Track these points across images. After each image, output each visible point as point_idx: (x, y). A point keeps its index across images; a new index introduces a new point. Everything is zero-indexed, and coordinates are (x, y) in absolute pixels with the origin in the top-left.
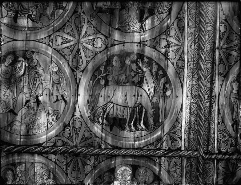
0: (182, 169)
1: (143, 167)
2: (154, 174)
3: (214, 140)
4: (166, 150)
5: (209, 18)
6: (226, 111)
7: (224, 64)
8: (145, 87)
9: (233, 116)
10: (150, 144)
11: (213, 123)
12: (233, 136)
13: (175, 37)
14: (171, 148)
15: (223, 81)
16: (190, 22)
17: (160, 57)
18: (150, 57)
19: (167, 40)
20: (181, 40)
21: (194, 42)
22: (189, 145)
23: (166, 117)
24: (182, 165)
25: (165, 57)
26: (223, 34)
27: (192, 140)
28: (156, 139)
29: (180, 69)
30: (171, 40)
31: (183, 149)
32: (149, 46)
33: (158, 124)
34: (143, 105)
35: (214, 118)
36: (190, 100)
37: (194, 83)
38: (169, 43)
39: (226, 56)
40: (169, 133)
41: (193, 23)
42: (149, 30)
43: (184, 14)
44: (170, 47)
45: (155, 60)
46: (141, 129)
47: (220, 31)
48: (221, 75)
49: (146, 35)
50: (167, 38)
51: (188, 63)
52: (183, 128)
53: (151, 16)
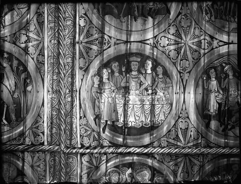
0: (45, 163)
1: (7, 162)
2: (18, 169)
3: (76, 134)
4: (28, 145)
5: (68, 11)
6: (87, 106)
7: (84, 59)
8: (6, 83)
9: (94, 111)
10: (13, 140)
11: (75, 117)
12: (95, 130)
13: (34, 32)
14: (34, 143)
15: (83, 75)
16: (50, 17)
17: (20, 52)
18: (10, 52)
19: (27, 35)
20: (41, 35)
21: (53, 36)
22: (51, 140)
23: (27, 112)
24: (45, 160)
25: (25, 53)
26: (82, 29)
27: (55, 135)
28: (18, 134)
29: (41, 64)
30: (31, 35)
31: (46, 143)
32: (9, 41)
33: (20, 119)
34: (4, 101)
35: (76, 113)
36: (51, 95)
37: (55, 77)
38: (29, 38)
39: (87, 50)
40: (31, 128)
41: (53, 18)
42: (9, 25)
43: (43, 9)
44: (29, 42)
45: (16, 56)
46: (4, 124)
47: (79, 25)
48: (82, 69)
49: (6, 31)
50: (27, 33)
51: (48, 58)
52: (45, 123)
53: (11, 12)
